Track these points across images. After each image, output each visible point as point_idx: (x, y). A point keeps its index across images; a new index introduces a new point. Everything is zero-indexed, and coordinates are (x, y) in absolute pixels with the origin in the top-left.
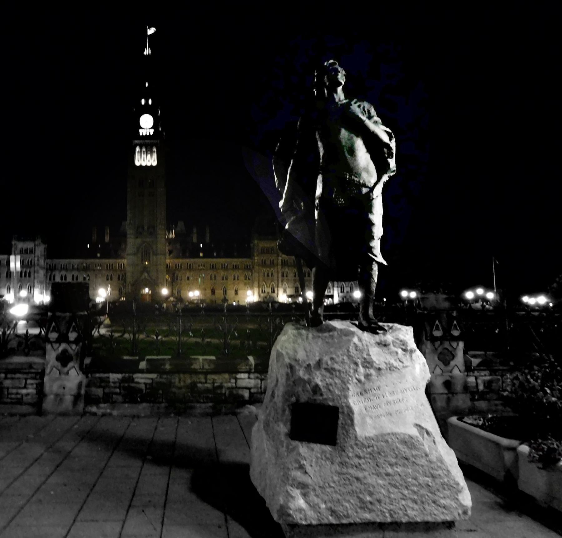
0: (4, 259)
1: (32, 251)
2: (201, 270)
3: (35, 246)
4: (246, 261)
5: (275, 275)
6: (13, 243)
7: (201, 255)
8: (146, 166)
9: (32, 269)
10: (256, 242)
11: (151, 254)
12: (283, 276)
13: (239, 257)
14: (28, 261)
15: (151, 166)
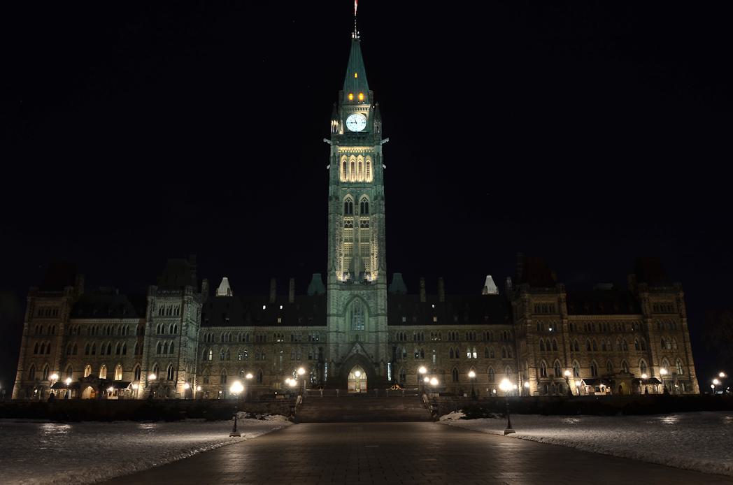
0: (133, 326)
1: (179, 312)
2: (434, 342)
3: (184, 302)
4: (502, 328)
5: (560, 347)
6: (149, 299)
7: (435, 319)
8: (357, 183)
9: (177, 339)
10: (527, 296)
11: (366, 314)
12: (572, 350)
13: (490, 322)
14: (172, 327)
15: (364, 183)
